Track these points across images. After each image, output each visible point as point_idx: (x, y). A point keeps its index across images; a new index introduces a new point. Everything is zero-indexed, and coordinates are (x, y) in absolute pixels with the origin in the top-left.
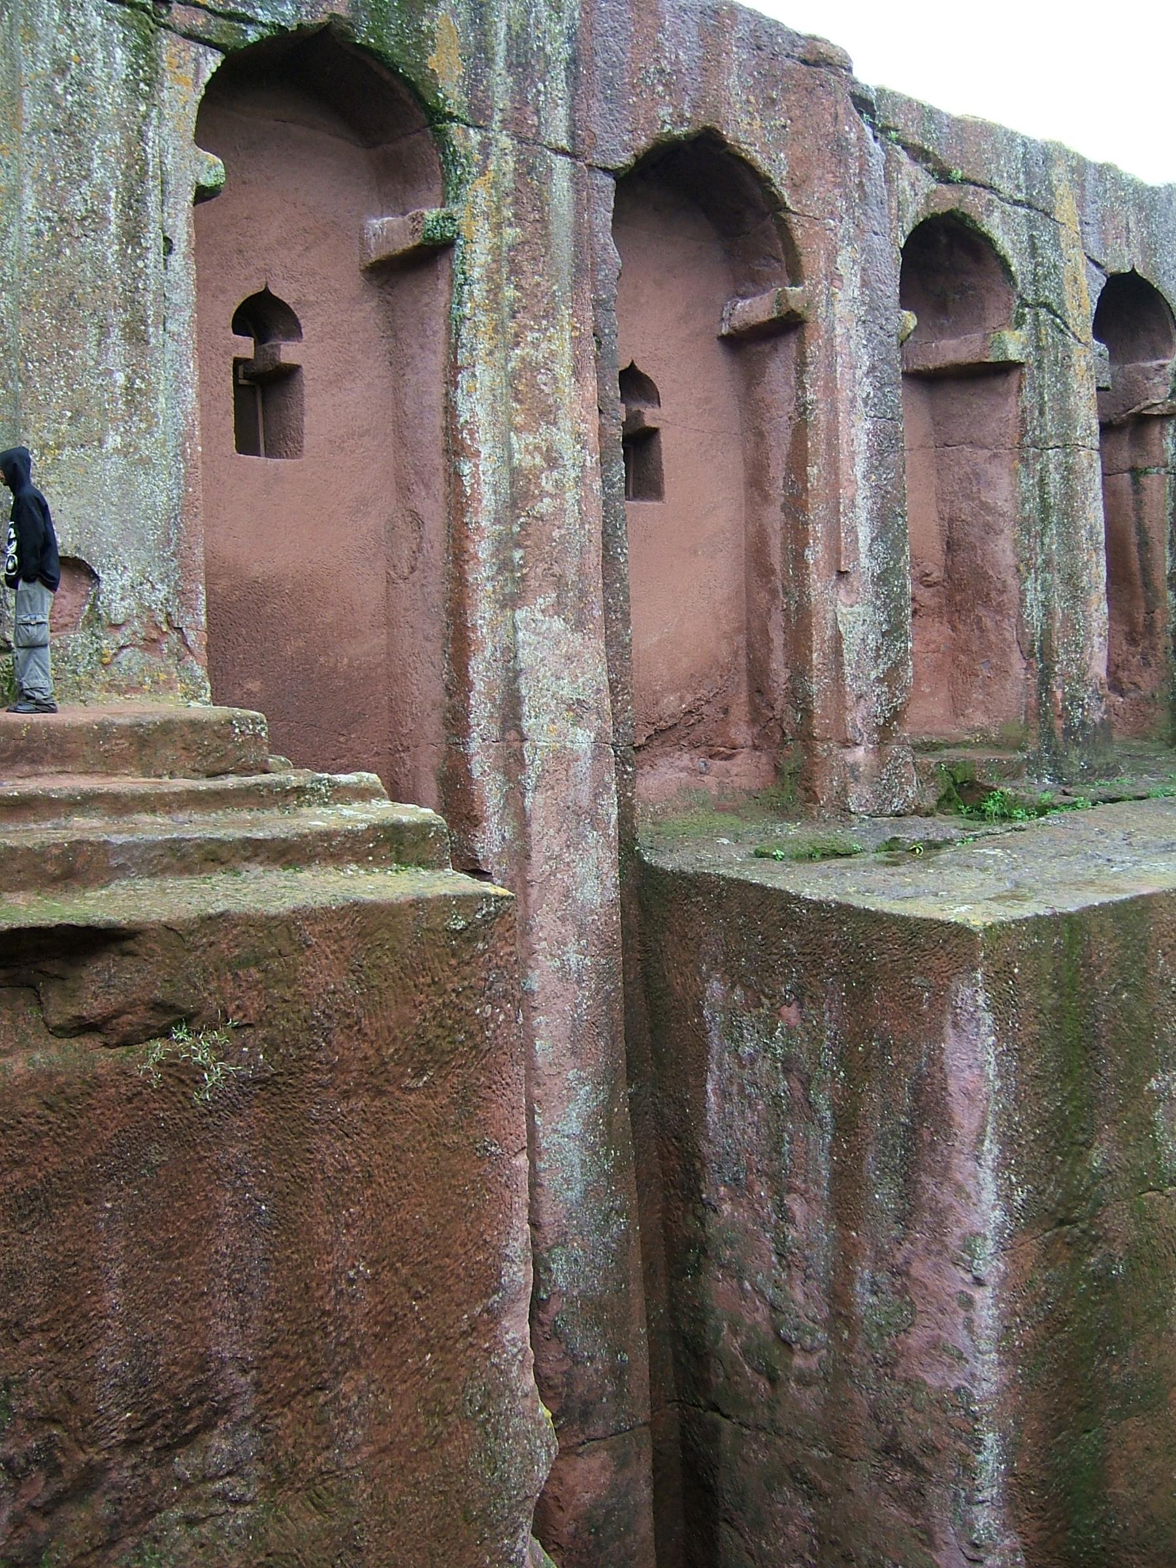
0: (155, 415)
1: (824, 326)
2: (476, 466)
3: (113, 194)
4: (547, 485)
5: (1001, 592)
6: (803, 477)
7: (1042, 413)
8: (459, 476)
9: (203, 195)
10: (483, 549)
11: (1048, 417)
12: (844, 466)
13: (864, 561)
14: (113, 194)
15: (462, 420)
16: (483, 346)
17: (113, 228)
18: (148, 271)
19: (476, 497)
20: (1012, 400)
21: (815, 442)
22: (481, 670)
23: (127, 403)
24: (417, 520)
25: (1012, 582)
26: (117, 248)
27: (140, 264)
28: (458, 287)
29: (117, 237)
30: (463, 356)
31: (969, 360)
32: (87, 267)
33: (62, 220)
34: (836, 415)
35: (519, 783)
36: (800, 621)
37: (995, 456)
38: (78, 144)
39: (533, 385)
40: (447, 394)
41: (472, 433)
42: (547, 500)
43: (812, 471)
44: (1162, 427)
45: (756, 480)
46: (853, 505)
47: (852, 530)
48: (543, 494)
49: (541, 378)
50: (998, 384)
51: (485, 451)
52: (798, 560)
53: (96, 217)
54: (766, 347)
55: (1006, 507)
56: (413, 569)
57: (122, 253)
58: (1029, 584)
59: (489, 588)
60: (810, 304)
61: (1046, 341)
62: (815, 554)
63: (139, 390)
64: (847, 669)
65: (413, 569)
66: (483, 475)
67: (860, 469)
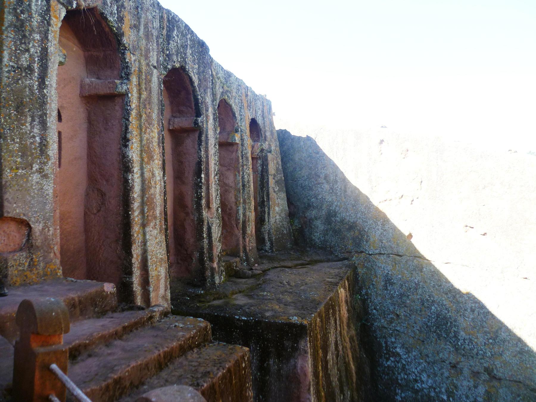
2: (133, 176)
3: (36, 59)
4: (153, 183)
5: (230, 210)
6: (201, 178)
7: (242, 158)
10: (136, 205)
13: (214, 204)
14: (36, 59)
16: (135, 133)
17: (36, 74)
18: (48, 94)
19: (133, 187)
20: (234, 153)
22: (136, 251)
23: (40, 150)
24: (103, 195)
25: (234, 207)
27: (45, 91)
30: (129, 136)
31: (223, 141)
32: (27, 89)
33: (18, 68)
36: (199, 223)
37: (229, 169)
38: (24, 36)
39: (148, 147)
40: (120, 149)
41: (132, 163)
43: (203, 176)
44: (257, 161)
45: (179, 177)
47: (212, 195)
50: (230, 148)
52: (199, 205)
53: (30, 69)
54: (185, 135)
55: (232, 184)
56: (99, 211)
57: (39, 85)
58: (239, 208)
60: (202, 122)
62: (203, 202)
63: (44, 145)
65: (99, 211)
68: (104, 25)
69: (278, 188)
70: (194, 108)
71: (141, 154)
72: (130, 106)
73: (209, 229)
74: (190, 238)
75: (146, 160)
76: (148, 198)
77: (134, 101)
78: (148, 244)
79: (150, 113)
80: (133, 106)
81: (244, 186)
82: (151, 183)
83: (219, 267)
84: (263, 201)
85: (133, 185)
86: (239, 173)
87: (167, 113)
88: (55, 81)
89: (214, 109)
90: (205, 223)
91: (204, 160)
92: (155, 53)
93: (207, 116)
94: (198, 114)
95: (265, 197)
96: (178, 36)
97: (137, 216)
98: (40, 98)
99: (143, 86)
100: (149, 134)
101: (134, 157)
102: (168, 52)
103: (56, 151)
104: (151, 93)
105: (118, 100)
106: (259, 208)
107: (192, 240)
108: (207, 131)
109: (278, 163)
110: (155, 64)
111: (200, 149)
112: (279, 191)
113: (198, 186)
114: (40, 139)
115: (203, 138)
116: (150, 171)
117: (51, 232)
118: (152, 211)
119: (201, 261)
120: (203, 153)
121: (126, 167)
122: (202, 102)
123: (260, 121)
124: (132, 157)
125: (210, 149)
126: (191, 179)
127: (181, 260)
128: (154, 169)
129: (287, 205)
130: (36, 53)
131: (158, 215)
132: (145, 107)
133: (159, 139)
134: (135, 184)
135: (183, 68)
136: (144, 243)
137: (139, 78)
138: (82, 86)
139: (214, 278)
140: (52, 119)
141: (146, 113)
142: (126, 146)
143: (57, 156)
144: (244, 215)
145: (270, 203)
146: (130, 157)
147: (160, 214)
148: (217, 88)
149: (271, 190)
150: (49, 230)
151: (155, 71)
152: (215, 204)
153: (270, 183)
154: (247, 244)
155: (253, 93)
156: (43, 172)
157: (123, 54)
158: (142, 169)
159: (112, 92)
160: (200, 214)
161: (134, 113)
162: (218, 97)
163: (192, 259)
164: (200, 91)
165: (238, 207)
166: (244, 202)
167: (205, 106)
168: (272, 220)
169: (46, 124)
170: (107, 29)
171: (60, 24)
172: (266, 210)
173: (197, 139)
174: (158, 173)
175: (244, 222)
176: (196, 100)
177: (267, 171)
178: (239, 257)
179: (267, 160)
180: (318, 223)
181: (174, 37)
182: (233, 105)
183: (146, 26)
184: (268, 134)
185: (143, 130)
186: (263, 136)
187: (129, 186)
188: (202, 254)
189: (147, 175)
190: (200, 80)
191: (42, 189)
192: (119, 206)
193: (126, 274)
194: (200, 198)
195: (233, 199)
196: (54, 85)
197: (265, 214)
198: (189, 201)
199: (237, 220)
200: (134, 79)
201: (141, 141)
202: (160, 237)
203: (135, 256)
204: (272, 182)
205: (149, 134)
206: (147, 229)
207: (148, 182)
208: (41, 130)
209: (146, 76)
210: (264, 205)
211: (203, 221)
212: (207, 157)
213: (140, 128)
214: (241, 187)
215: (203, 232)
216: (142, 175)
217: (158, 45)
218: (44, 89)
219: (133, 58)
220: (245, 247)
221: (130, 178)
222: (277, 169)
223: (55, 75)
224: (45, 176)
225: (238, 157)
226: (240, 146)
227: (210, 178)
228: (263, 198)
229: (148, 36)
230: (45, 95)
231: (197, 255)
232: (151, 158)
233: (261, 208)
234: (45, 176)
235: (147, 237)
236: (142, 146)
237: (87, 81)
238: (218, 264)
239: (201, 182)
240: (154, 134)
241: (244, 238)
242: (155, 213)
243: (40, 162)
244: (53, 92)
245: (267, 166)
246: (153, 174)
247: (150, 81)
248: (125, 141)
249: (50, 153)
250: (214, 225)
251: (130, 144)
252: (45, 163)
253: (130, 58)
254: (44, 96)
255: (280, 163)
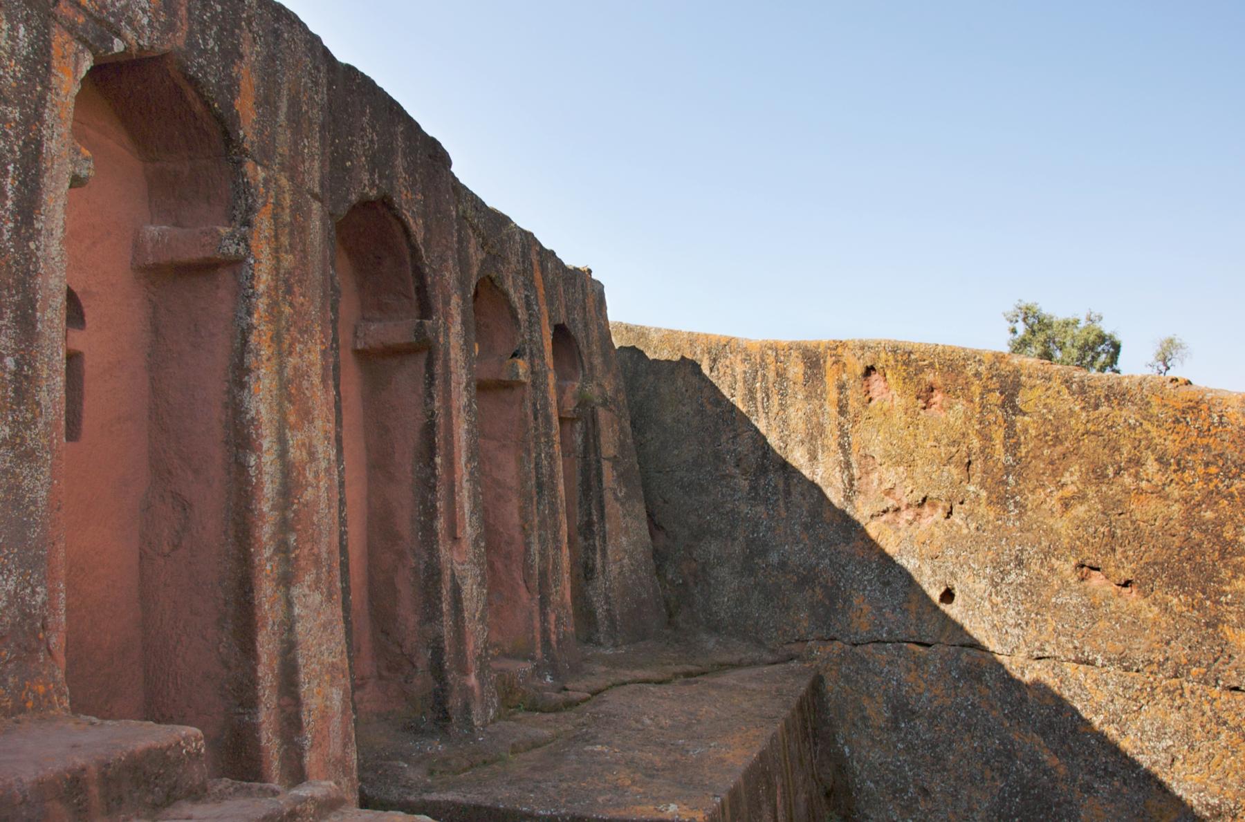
0: (38, 404)
1: (442, 349)
2: (259, 457)
3: (10, 168)
4: (310, 476)
6: (433, 467)
7: (536, 419)
8: (242, 467)
9: (77, 181)
10: (266, 531)
11: (540, 420)
12: (456, 455)
13: (468, 528)
14: (10, 168)
15: (248, 417)
16: (265, 353)
17: (9, 203)
18: (39, 254)
19: (259, 486)
21: (439, 439)
22: (267, 645)
23: (16, 391)
24: (185, 506)
26: (11, 225)
27: (32, 245)
28: (245, 296)
29: (12, 213)
30: (250, 360)
34: (451, 418)
35: (295, 744)
37: (504, 446)
39: (299, 388)
40: (229, 392)
41: (257, 428)
42: (310, 489)
43: (438, 460)
45: (379, 464)
46: (462, 487)
47: (462, 507)
48: (308, 484)
49: (305, 384)
51: (266, 444)
52: (429, 531)
56: (175, 547)
57: (16, 230)
59: (268, 568)
61: (537, 368)
62: (440, 524)
63: (26, 377)
64: (466, 614)
65: (175, 547)
66: (265, 464)
67: (463, 460)
68: (191, 94)
69: (624, 490)
70: (415, 297)
71: (280, 405)
72: (252, 287)
73: (457, 591)
74: (408, 614)
75: (292, 419)
76: (296, 513)
77: (264, 277)
78: (299, 627)
79: (302, 305)
80: (261, 288)
81: (540, 485)
82: (305, 477)
83: (482, 685)
84: (589, 524)
85: (259, 482)
86: (529, 455)
87: (349, 308)
88: (61, 223)
89: (464, 298)
90: (447, 577)
91: (440, 420)
92: (317, 164)
93: (447, 316)
94: (425, 309)
95: (594, 512)
96: (373, 127)
97: (269, 559)
98: (17, 262)
99: (285, 240)
100: (301, 356)
101: (263, 411)
102: (349, 164)
103: (60, 394)
104: (306, 257)
105: (225, 276)
106: (580, 539)
107: (413, 620)
108: (447, 353)
109: (622, 430)
110: (317, 190)
111: (431, 396)
112: (628, 497)
113: (427, 485)
114: (17, 363)
115: (438, 369)
116: (304, 444)
117: (39, 599)
118: (308, 546)
119: (437, 669)
120: (437, 404)
121: (240, 438)
122: (433, 282)
123: (578, 332)
124: (258, 412)
125: (454, 395)
126: (409, 468)
127: (389, 669)
128: (315, 442)
129: (647, 532)
130: (12, 151)
131: (324, 555)
132: (289, 291)
133: (324, 368)
134: (266, 478)
135: (386, 202)
136: (289, 624)
137: (275, 217)
138: (138, 246)
139: (469, 713)
140: (49, 314)
141: (291, 305)
142: (242, 386)
143: (62, 408)
144: (543, 556)
145: (607, 526)
146: (253, 413)
147: (330, 552)
148: (472, 251)
149: (608, 496)
150: (34, 592)
151: (316, 206)
152: (468, 531)
153: (604, 479)
154: (552, 627)
155: (559, 263)
156: (21, 445)
157: (240, 164)
158: (282, 441)
159: (209, 254)
160: (433, 553)
161: (262, 304)
162: (475, 270)
163: (414, 666)
164: (428, 257)
165: (528, 536)
166: (543, 522)
167: (443, 293)
168: (614, 569)
169: (34, 327)
170: (198, 107)
171: (76, 90)
172: (597, 544)
173: (424, 370)
174: (325, 451)
175: (543, 574)
176: (420, 276)
177: (597, 449)
178: (533, 659)
179: (595, 421)
180: (723, 572)
181: (363, 129)
182: (512, 291)
183: (294, 103)
184: (597, 361)
185: (286, 346)
186: (586, 366)
187: (249, 483)
188: (438, 651)
189: (295, 454)
190: (427, 228)
191: (19, 487)
192: (225, 532)
193: (241, 705)
194: (431, 513)
195: (516, 519)
196: (58, 233)
197: (594, 554)
198: (405, 522)
199: (527, 567)
200: (263, 222)
201: (280, 372)
202: (329, 612)
203: (264, 658)
204: (609, 475)
205: (301, 356)
206: (295, 591)
207: (299, 474)
208: (18, 341)
209: (293, 216)
210: (592, 532)
211: (439, 573)
212: (448, 415)
213: (277, 338)
214: (534, 491)
215: (440, 599)
216: (283, 453)
217: (323, 145)
218: (30, 238)
219: (261, 174)
220: (545, 632)
221: (252, 463)
222: (622, 445)
223: (60, 210)
224: (28, 456)
225: (526, 415)
226: (529, 388)
227: (456, 466)
228: (590, 514)
229: (296, 119)
230: (32, 253)
231: (424, 658)
232: (306, 415)
233: (586, 539)
234: (28, 456)
235: (297, 611)
236: (284, 385)
237: (153, 230)
238: (478, 676)
239: (434, 475)
240: (311, 356)
241: (544, 614)
242: (316, 550)
243: (14, 421)
244: (55, 248)
245: (596, 437)
246: (312, 455)
247: (303, 230)
248: (240, 374)
249: (43, 397)
250: (469, 581)
251: (250, 380)
252: (27, 425)
253: (256, 173)
254: (30, 257)
255: (629, 430)
